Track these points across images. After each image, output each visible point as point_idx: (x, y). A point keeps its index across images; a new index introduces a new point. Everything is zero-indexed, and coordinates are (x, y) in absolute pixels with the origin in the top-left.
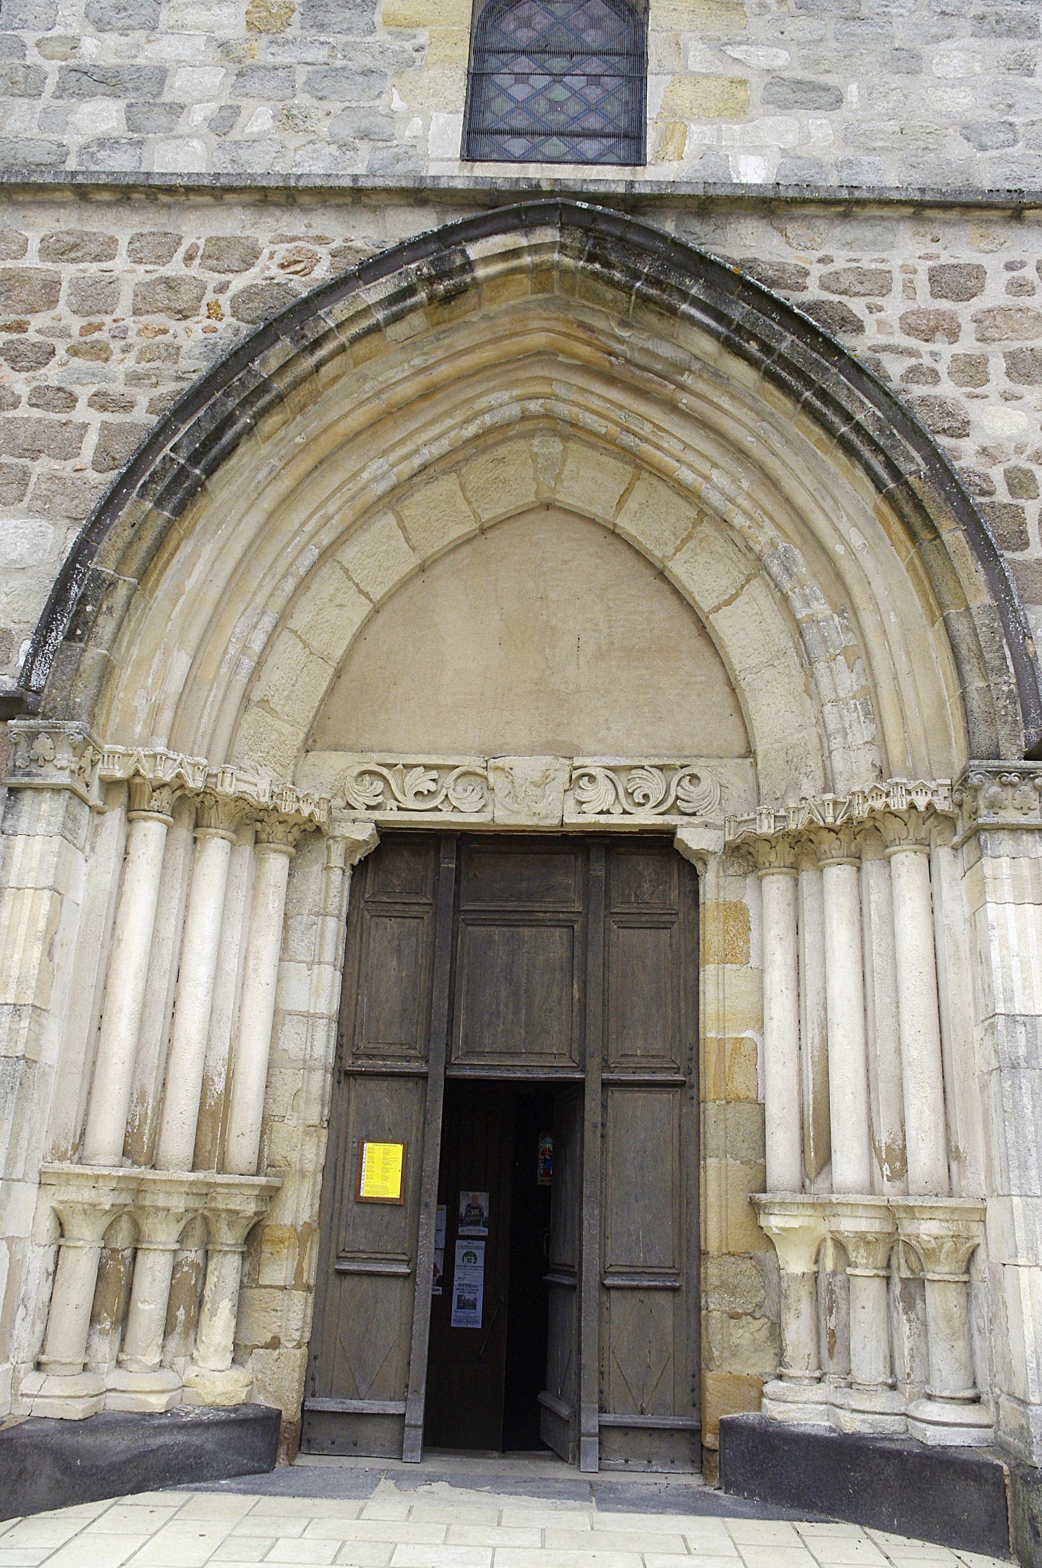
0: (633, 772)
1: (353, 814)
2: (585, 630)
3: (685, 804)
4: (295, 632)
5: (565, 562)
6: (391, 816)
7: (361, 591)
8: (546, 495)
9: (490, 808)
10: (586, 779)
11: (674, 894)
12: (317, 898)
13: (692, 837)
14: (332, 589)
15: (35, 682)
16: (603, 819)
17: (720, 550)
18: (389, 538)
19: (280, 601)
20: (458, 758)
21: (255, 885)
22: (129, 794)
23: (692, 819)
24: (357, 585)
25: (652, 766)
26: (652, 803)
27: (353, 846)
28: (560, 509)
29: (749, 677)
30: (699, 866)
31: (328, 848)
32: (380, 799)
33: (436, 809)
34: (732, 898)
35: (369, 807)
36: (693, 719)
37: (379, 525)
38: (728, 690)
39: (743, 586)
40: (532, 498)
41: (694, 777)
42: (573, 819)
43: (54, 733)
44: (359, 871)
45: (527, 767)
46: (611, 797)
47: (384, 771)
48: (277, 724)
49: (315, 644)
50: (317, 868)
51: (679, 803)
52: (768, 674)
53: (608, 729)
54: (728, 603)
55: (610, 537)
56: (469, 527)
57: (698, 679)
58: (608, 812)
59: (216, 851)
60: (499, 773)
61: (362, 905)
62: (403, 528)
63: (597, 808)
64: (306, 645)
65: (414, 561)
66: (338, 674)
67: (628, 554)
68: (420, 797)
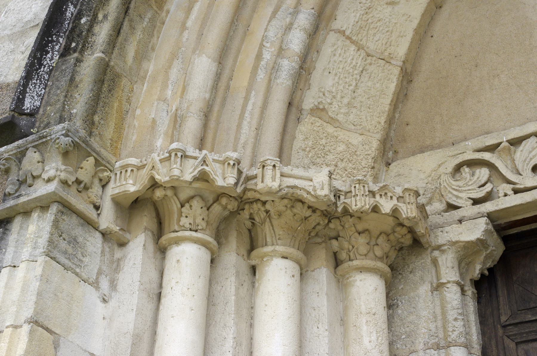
1: (456, 214)
4: (343, 33)
6: (506, 201)
12: (432, 326)
15: (28, 104)
21: (342, 320)
22: (150, 211)
27: (467, 252)
31: (435, 262)
32: (488, 187)
35: (476, 202)
43: (41, 146)
44: (484, 287)
47: (486, 156)
48: (342, 135)
49: (372, 46)
50: (424, 289)
59: (278, 276)
61: (500, 331)
64: (360, 48)
66: (407, 77)
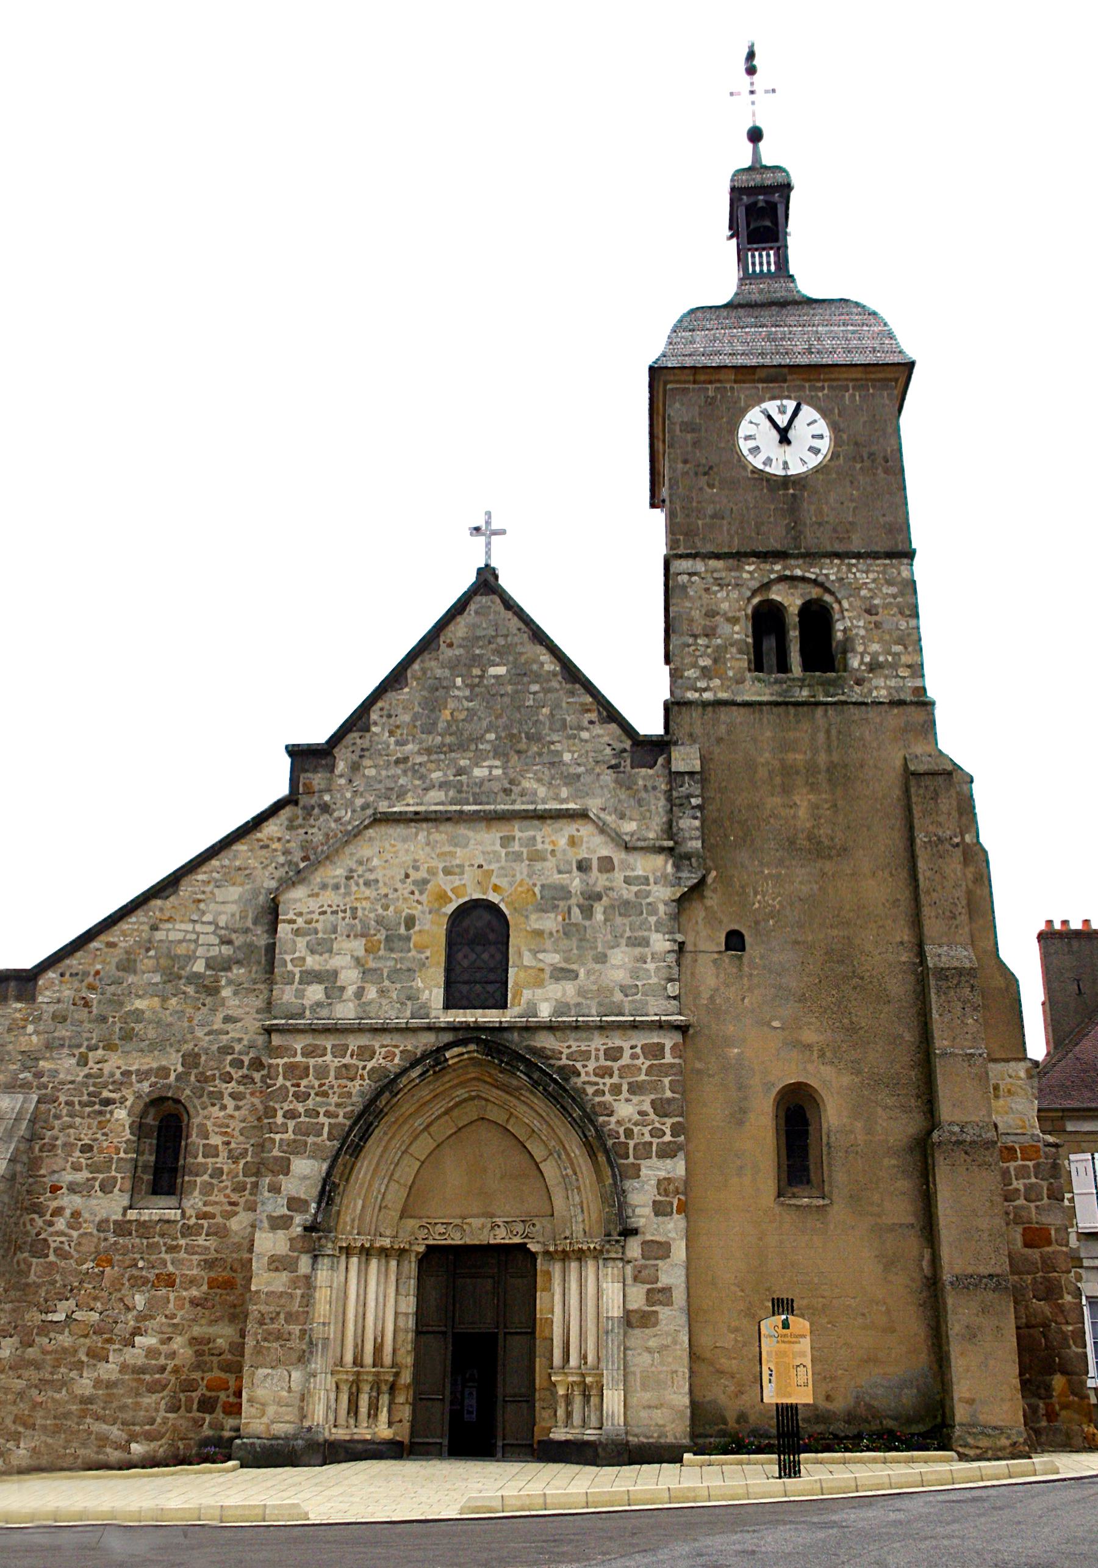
15: (319, 1220)
21: (387, 1270)
22: (348, 1251)
41: (534, 1225)
43: (326, 1237)
44: (420, 1262)
45: (476, 1222)
59: (374, 1263)
63: (501, 1237)
65: (435, 1144)
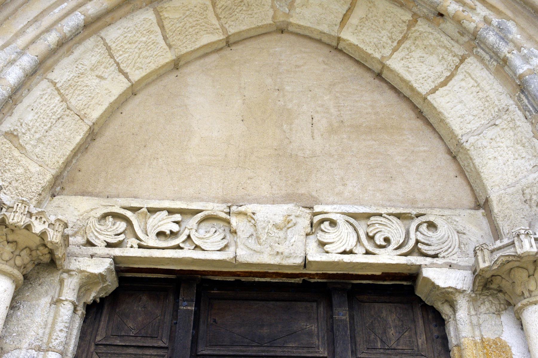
0: (372, 218)
1: (91, 250)
2: (317, 112)
3: (426, 247)
4: (55, 84)
5: (297, 66)
6: (130, 251)
7: (121, 71)
8: (281, 19)
9: (232, 249)
10: (327, 223)
11: (421, 340)
12: (41, 332)
13: (441, 276)
14: (94, 60)
16: (347, 258)
17: (434, 43)
18: (150, 32)
19: (41, 47)
20: (202, 204)
23: (435, 260)
24: (118, 64)
25: (390, 214)
26: (394, 244)
27: (89, 281)
28: (293, 33)
29: (472, 140)
30: (445, 310)
31: (61, 282)
32: (122, 237)
33: (178, 247)
34: (489, 335)
35: (109, 245)
36: (423, 176)
37: (142, 17)
38: (449, 157)
39: (457, 67)
40: (270, 21)
41: (432, 225)
42: (316, 256)
44: (93, 312)
45: (269, 213)
46: (353, 240)
47: (129, 214)
48: (24, 161)
49: (73, 102)
50: (45, 301)
51: (420, 246)
52: (491, 133)
53: (344, 185)
54: (444, 84)
55: (334, 52)
56: (218, 37)
57: (422, 149)
58: (351, 252)
60: (242, 218)
61: (93, 348)
62: (162, 27)
63: (340, 248)
64: (64, 100)
65: (169, 57)
66: (92, 135)
67: (349, 63)
68: (163, 238)
